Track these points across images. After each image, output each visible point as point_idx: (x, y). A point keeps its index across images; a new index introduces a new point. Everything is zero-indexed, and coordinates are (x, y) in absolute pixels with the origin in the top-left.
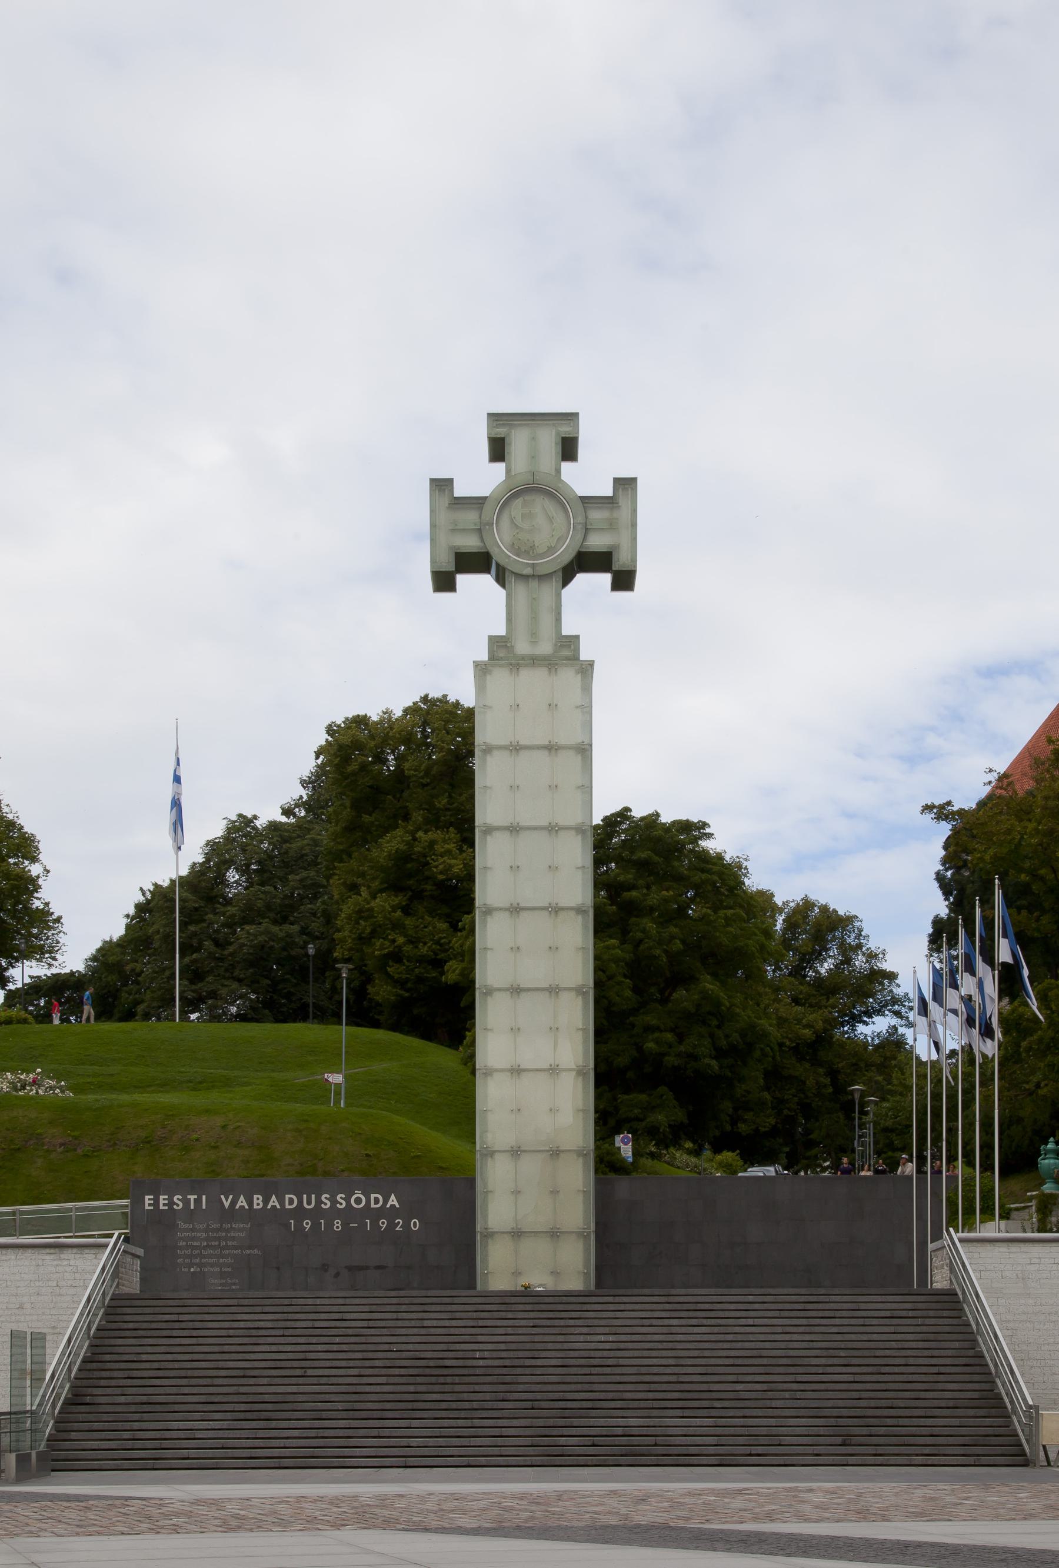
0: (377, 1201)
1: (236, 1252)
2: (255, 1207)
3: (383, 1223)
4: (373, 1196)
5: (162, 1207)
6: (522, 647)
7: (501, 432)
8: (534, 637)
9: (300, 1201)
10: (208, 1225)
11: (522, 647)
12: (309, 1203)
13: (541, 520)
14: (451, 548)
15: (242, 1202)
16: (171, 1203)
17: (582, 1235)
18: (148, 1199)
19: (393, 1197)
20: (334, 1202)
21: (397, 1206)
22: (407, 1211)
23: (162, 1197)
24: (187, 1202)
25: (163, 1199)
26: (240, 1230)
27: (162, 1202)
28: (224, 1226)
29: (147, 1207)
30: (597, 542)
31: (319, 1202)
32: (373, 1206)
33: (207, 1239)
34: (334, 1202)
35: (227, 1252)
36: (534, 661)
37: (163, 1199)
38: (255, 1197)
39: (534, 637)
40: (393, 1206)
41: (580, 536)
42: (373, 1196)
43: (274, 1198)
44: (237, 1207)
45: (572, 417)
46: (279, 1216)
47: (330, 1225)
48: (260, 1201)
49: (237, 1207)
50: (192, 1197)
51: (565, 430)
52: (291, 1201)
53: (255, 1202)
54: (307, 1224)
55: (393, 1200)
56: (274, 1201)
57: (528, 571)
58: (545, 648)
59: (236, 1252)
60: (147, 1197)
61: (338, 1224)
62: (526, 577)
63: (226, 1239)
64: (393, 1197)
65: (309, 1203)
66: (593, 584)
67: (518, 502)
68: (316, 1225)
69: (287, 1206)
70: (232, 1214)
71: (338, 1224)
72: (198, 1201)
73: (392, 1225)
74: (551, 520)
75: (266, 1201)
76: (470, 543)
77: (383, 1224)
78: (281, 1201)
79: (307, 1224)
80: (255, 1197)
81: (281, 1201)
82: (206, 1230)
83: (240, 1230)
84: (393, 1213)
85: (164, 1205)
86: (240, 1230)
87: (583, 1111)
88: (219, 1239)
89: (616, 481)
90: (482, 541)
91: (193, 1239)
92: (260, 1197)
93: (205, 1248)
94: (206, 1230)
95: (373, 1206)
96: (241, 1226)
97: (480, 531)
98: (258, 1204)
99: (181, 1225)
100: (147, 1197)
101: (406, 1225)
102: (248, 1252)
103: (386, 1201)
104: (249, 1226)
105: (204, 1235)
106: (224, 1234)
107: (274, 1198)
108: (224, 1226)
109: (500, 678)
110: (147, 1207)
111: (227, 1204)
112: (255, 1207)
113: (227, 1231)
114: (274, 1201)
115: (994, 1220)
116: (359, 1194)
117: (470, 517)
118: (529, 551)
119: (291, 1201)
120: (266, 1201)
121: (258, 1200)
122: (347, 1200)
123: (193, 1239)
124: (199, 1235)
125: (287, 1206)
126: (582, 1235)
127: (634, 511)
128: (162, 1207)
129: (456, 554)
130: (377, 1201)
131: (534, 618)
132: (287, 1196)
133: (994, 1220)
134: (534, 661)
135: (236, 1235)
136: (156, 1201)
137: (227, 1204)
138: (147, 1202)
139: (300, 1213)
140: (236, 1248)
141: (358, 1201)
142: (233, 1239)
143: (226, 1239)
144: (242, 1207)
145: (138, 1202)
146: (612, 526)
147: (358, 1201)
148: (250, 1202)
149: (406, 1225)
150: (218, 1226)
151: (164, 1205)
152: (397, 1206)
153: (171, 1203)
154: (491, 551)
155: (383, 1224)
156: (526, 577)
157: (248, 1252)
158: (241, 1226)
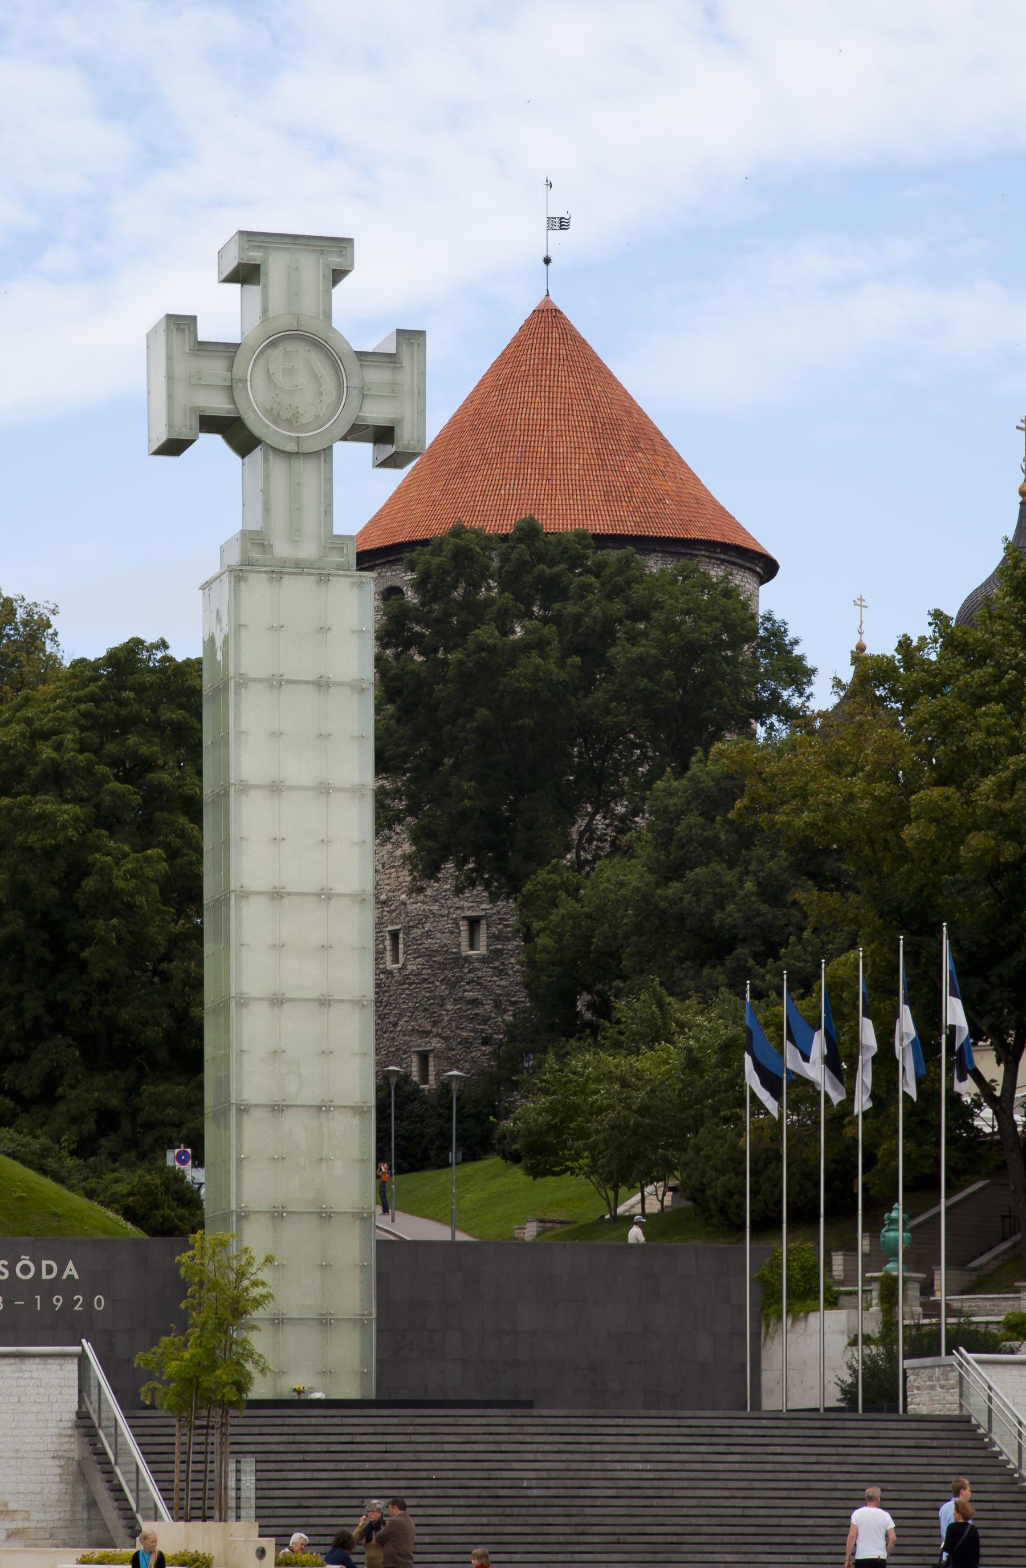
0: (49, 1270)
3: (58, 1300)
4: (44, 1263)
6: (282, 549)
7: (255, 256)
8: (295, 533)
11: (282, 549)
13: (303, 379)
14: (194, 409)
17: (360, 1323)
19: (70, 1265)
21: (76, 1277)
22: (90, 1284)
30: (376, 413)
32: (44, 1276)
36: (299, 568)
39: (295, 533)
42: (44, 1263)
45: (343, 245)
51: (335, 261)
57: (291, 447)
58: (308, 551)
62: (289, 455)
64: (70, 1265)
67: (277, 353)
73: (69, 1303)
74: (317, 379)
76: (217, 404)
77: (58, 1301)
84: (68, 1287)
87: (363, 1160)
89: (400, 332)
90: (233, 400)
95: (44, 1276)
97: (230, 389)
101: (88, 1303)
103: (61, 1270)
109: (257, 585)
115: (818, 1310)
116: (25, 1261)
117: (215, 368)
118: (292, 421)
126: (360, 1323)
127: (422, 374)
129: (200, 416)
130: (49, 1270)
131: (295, 508)
133: (818, 1310)
134: (299, 568)
141: (25, 1270)
146: (394, 391)
147: (25, 1270)
152: (76, 1277)
154: (244, 417)
155: (58, 1301)
156: (289, 455)
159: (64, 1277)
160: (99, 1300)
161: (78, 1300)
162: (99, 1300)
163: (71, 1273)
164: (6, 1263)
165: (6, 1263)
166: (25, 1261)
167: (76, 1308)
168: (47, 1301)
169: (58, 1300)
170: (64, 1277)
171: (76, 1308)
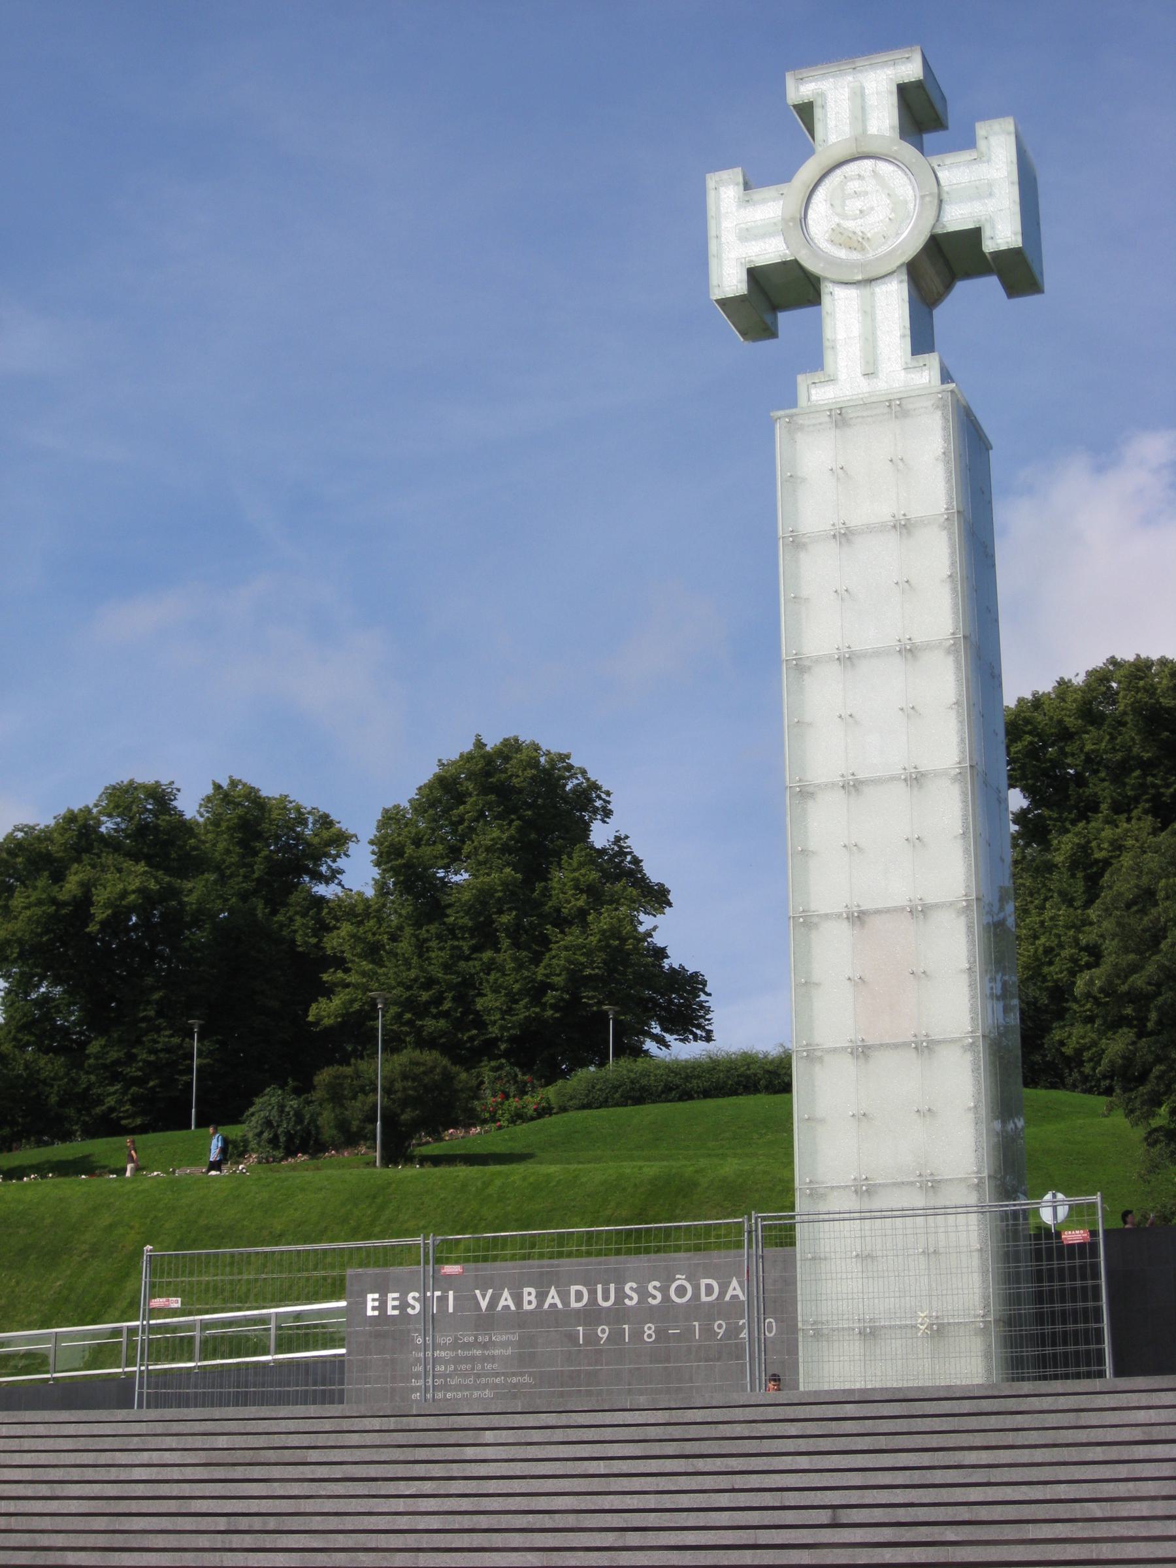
0: (709, 1288)
1: (497, 1380)
2: (526, 1307)
3: (720, 1326)
4: (704, 1282)
5: (390, 1312)
9: (593, 1293)
10: (456, 1339)
12: (606, 1299)
15: (506, 1300)
16: (403, 1306)
18: (372, 1300)
20: (643, 1294)
23: (391, 1296)
26: (504, 1342)
27: (390, 1303)
28: (480, 1339)
29: (370, 1313)
31: (621, 1295)
32: (704, 1298)
33: (457, 1361)
34: (643, 1294)
35: (484, 1380)
42: (704, 1282)
43: (553, 1291)
44: (499, 1308)
47: (637, 1335)
48: (532, 1298)
49: (499, 1308)
52: (578, 1296)
53: (526, 1298)
55: (735, 1289)
56: (553, 1298)
59: (497, 1380)
60: (370, 1297)
61: (649, 1330)
63: (484, 1359)
65: (606, 1299)
70: (489, 1320)
71: (649, 1330)
75: (542, 1297)
77: (720, 1327)
78: (564, 1296)
79: (603, 1332)
80: (526, 1290)
81: (564, 1296)
82: (455, 1346)
83: (504, 1345)
84: (730, 1310)
85: (394, 1308)
86: (504, 1345)
88: (472, 1359)
93: (450, 1376)
94: (455, 1346)
95: (704, 1298)
96: (504, 1338)
98: (530, 1303)
100: (370, 1297)
102: (515, 1380)
103: (724, 1288)
106: (478, 1352)
107: (553, 1291)
108: (480, 1339)
110: (370, 1313)
111: (484, 1304)
112: (526, 1307)
113: (485, 1346)
116: (681, 1280)
119: (578, 1296)
120: (542, 1297)
121: (529, 1295)
122: (664, 1290)
125: (574, 1305)
128: (390, 1312)
130: (709, 1288)
132: (574, 1288)
135: (497, 1352)
137: (484, 1304)
138: (370, 1304)
139: (592, 1315)
140: (497, 1375)
142: (493, 1359)
143: (484, 1359)
147: (681, 1291)
148: (518, 1299)
150: (472, 1339)
151: (394, 1308)
153: (403, 1306)
155: (720, 1327)
157: (515, 1380)
158: (504, 1338)
159: (727, 1298)
163: (735, 1293)
166: (681, 1280)
168: (708, 1331)
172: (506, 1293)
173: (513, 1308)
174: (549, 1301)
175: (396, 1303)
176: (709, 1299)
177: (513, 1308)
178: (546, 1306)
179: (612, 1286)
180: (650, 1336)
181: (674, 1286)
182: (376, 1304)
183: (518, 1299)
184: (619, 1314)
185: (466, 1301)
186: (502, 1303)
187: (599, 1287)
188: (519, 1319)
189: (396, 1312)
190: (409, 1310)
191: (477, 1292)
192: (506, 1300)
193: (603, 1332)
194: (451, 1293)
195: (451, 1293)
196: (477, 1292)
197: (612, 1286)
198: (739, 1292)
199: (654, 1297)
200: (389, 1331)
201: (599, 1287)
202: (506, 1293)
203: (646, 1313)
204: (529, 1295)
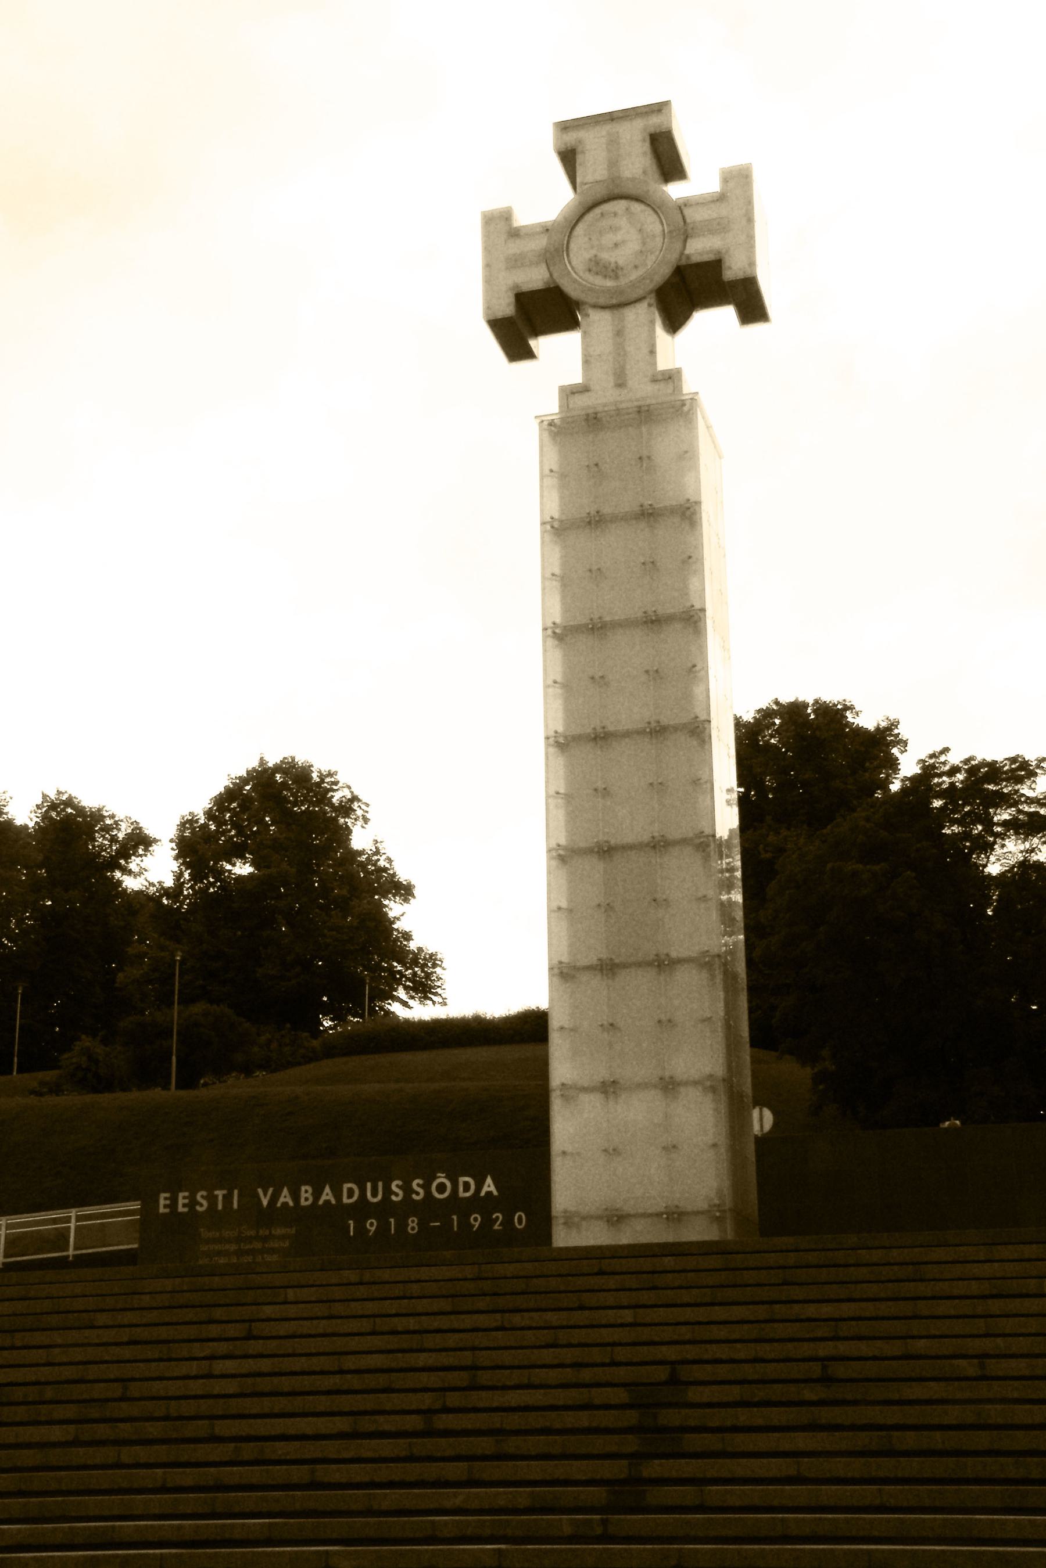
2: (303, 1203)
3: (476, 1219)
5: (181, 1209)
12: (374, 1194)
15: (285, 1197)
16: (193, 1203)
18: (163, 1199)
19: (489, 1180)
20: (407, 1189)
21: (495, 1193)
23: (181, 1195)
24: (212, 1199)
25: (182, 1198)
28: (261, 1232)
29: (162, 1210)
31: (388, 1192)
32: (462, 1194)
34: (407, 1189)
37: (182, 1198)
38: (303, 1188)
40: (489, 1193)
41: (678, 246)
43: (327, 1189)
44: (279, 1205)
45: (661, 108)
46: (336, 1213)
47: (402, 1226)
49: (279, 1205)
50: (220, 1193)
52: (350, 1193)
53: (303, 1195)
54: (372, 1224)
55: (489, 1186)
56: (327, 1195)
60: (163, 1195)
61: (413, 1224)
64: (489, 1180)
65: (374, 1194)
66: (714, 322)
68: (383, 1227)
69: (346, 1200)
70: (272, 1215)
71: (413, 1224)
72: (228, 1198)
75: (317, 1194)
76: (534, 278)
77: (476, 1220)
78: (337, 1193)
79: (372, 1225)
81: (338, 1195)
85: (184, 1205)
86: (283, 1238)
91: (219, 1253)
92: (309, 1189)
95: (462, 1194)
99: (204, 1233)
100: (163, 1195)
101: (508, 1222)
103: (479, 1189)
104: (293, 1231)
105: (233, 1247)
106: (258, 1245)
107: (327, 1189)
108: (261, 1232)
110: (162, 1210)
111: (265, 1202)
112: (303, 1203)
113: (265, 1239)
114: (327, 1195)
119: (350, 1193)
120: (317, 1194)
121: (306, 1193)
122: (426, 1186)
123: (219, 1253)
124: (227, 1247)
125: (346, 1200)
128: (181, 1209)
132: (346, 1186)
136: (174, 1200)
137: (265, 1202)
138: (162, 1202)
139: (362, 1209)
141: (441, 1188)
142: (272, 1251)
144: (285, 1204)
145: (150, 1202)
147: (441, 1188)
148: (296, 1195)
149: (508, 1222)
150: (252, 1233)
152: (495, 1193)
153: (193, 1203)
155: (476, 1220)
159: (483, 1194)
160: (520, 1218)
161: (497, 1217)
162: (520, 1218)
164: (420, 1182)
165: (420, 1182)
167: (496, 1227)
168: (464, 1224)
169: (476, 1219)
170: (483, 1194)
171: (496, 1227)
172: (285, 1191)
173: (291, 1204)
174: (324, 1197)
175: (186, 1201)
176: (467, 1195)
177: (291, 1204)
178: (321, 1202)
179: (380, 1184)
180: (413, 1229)
181: (434, 1185)
182: (168, 1202)
183: (296, 1195)
184: (385, 1208)
185: (250, 1198)
186: (282, 1200)
187: (369, 1185)
188: (296, 1215)
189: (186, 1210)
190: (198, 1208)
191: (260, 1191)
192: (285, 1197)
193: (372, 1225)
194: (236, 1192)
195: (236, 1192)
196: (260, 1191)
197: (380, 1184)
198: (492, 1188)
199: (418, 1194)
200: (181, 1226)
201: (369, 1185)
202: (285, 1191)
203: (408, 1206)
204: (306, 1193)
